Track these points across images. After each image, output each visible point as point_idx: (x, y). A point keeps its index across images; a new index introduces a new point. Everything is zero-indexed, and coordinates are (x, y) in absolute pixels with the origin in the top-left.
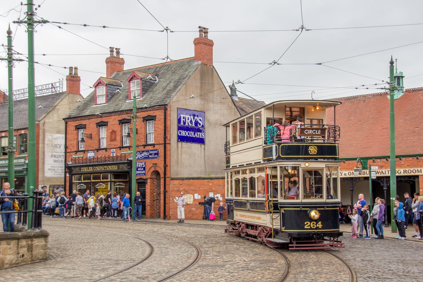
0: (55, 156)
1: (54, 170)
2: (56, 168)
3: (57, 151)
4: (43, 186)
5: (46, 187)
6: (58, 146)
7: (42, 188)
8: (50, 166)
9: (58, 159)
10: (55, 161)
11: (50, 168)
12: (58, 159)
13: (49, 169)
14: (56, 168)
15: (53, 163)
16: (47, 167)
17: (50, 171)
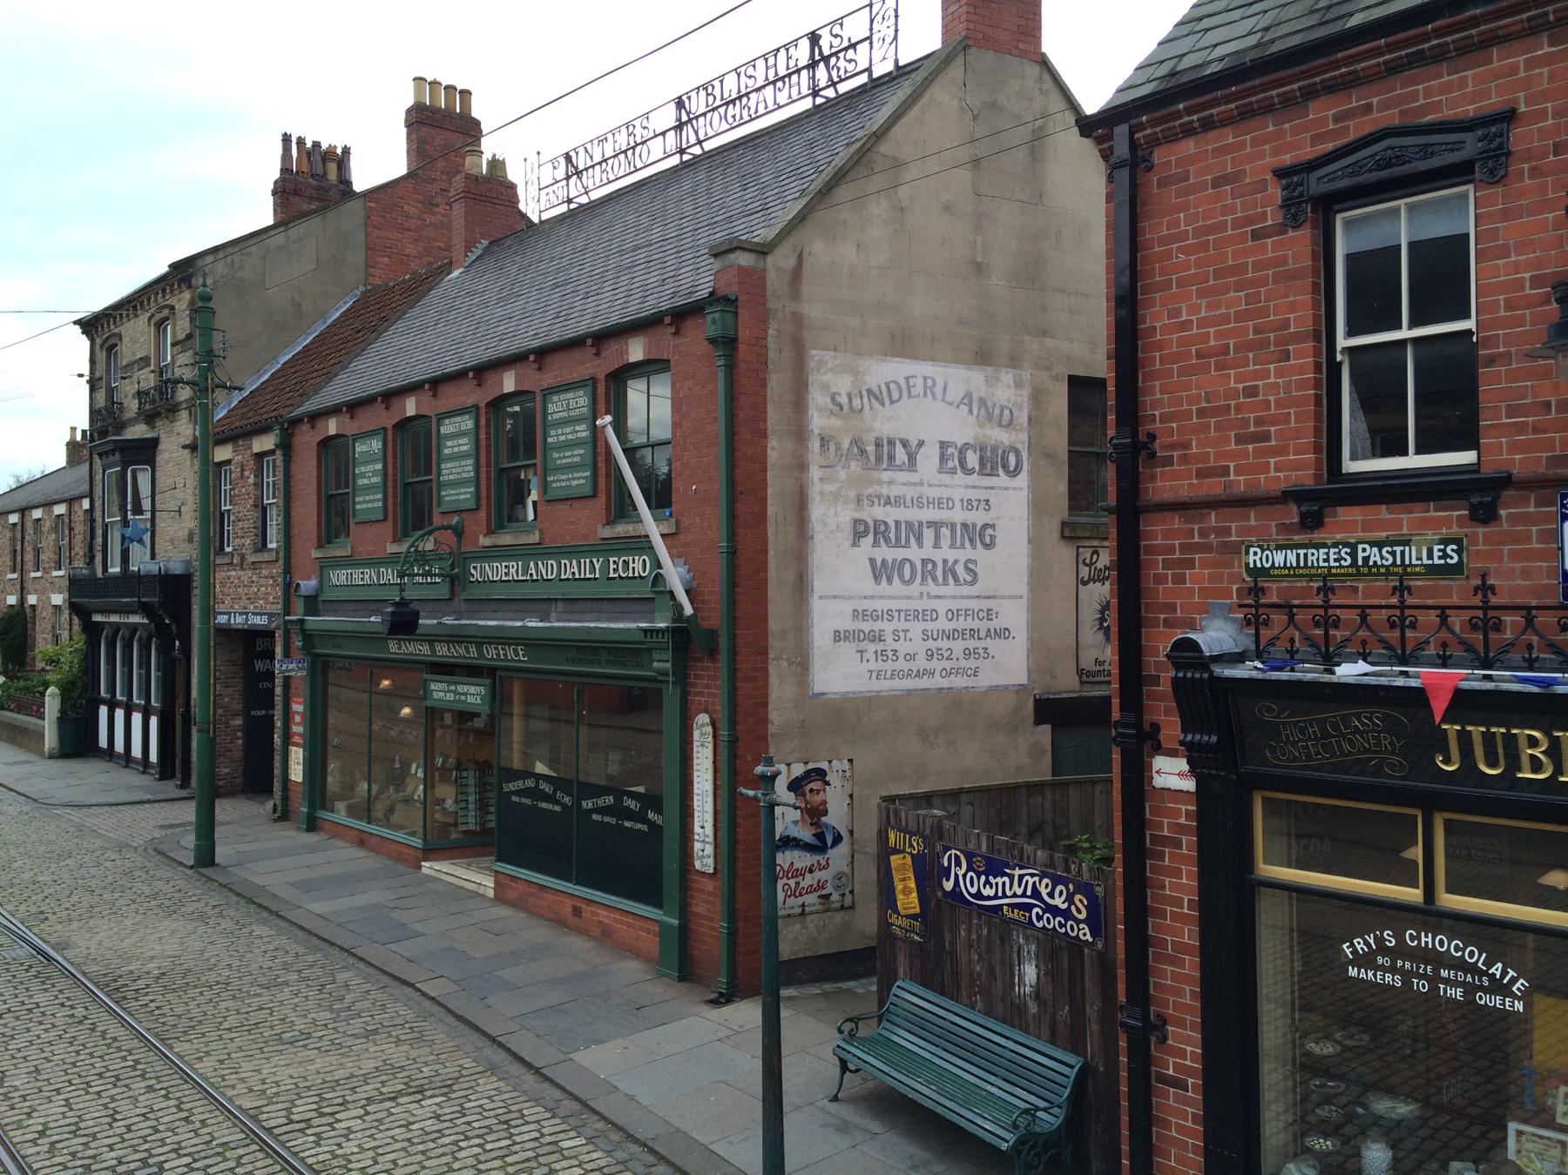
0: (879, 532)
1: (877, 637)
2: (888, 627)
3: (895, 491)
4: (798, 770)
5: (821, 774)
6: (901, 455)
7: (795, 786)
8: (848, 607)
9: (900, 554)
10: (880, 571)
11: (846, 623)
12: (900, 554)
13: (838, 637)
14: (888, 627)
15: (867, 584)
16: (826, 617)
17: (848, 650)
